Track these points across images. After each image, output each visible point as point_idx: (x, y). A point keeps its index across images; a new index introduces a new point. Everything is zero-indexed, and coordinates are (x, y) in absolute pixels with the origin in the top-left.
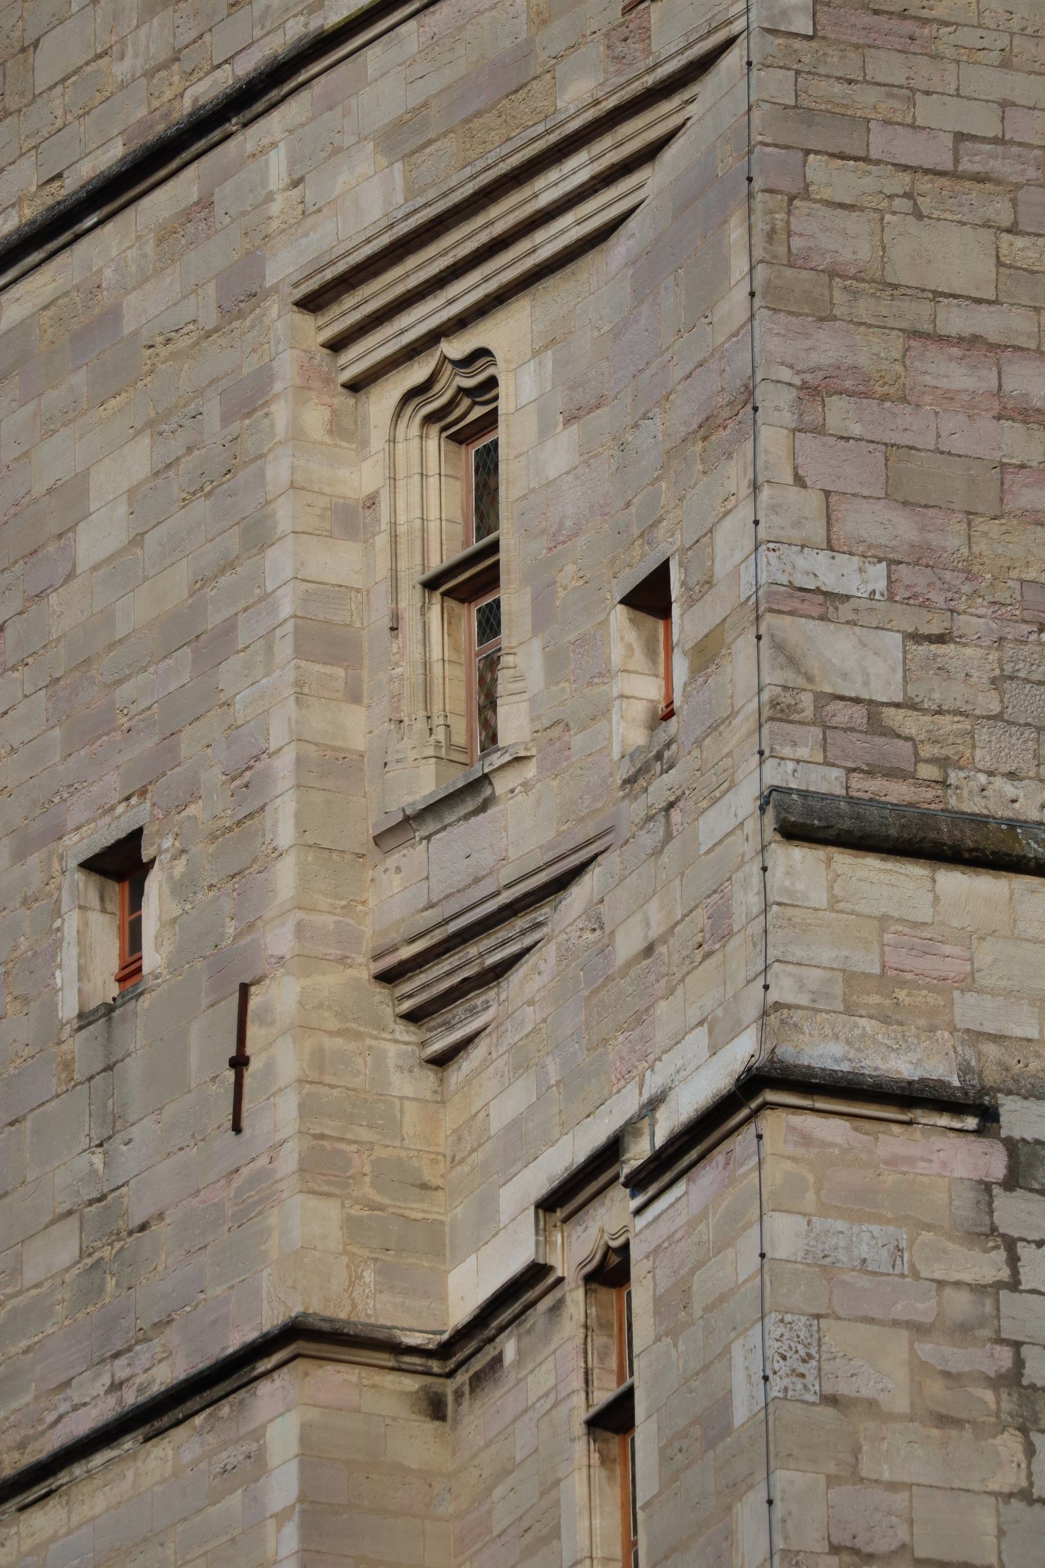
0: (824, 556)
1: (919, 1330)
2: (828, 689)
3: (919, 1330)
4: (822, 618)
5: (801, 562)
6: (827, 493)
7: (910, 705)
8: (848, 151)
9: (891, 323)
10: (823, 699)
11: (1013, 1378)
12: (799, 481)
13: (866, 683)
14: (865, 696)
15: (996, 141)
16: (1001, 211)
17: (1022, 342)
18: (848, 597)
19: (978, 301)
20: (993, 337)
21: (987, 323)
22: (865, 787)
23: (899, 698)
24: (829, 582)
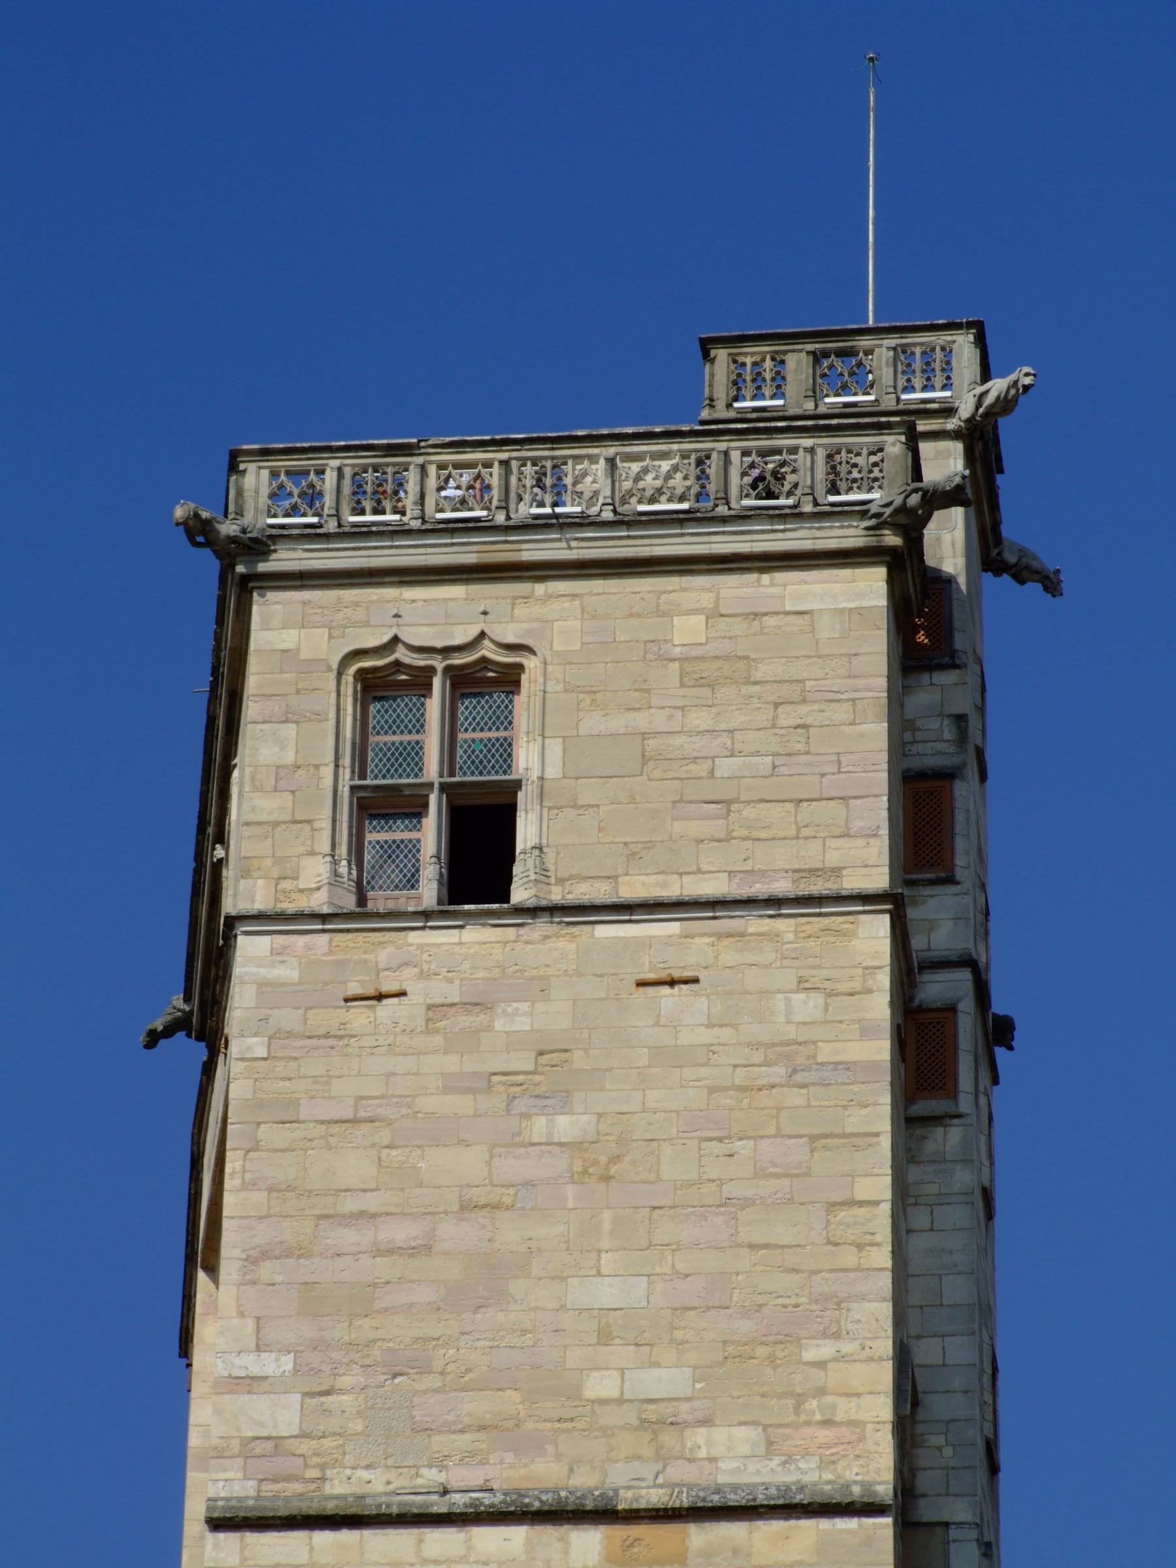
0: (252, 1356)
2: (250, 1434)
4: (249, 1393)
5: (237, 1362)
6: (258, 1319)
7: (304, 1435)
8: (286, 1119)
9: (307, 1212)
10: (247, 1442)
12: (242, 1314)
13: (275, 1427)
14: (275, 1434)
15: (382, 1097)
16: (384, 1136)
17: (392, 1209)
18: (267, 1377)
19: (364, 1191)
20: (373, 1209)
21: (371, 1203)
22: (270, 1489)
23: (296, 1432)
24: (255, 1371)
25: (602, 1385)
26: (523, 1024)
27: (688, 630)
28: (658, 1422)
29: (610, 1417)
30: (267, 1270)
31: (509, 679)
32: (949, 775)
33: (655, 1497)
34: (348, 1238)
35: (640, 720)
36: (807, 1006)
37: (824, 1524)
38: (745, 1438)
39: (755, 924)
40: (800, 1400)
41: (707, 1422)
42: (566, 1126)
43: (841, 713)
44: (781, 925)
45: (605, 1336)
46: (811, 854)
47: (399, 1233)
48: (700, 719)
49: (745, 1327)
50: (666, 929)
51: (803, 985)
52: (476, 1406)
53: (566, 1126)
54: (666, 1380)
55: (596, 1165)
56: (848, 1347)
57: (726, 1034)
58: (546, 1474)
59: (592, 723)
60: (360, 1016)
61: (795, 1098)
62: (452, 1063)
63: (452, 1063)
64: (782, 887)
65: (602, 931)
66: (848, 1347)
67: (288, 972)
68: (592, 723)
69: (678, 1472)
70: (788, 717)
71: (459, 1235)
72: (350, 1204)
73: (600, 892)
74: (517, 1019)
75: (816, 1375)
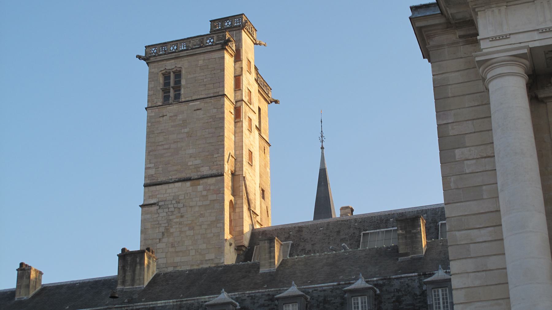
1: (151, 222)
3: (151, 222)
11: (158, 224)
21: (163, 143)
25: (190, 163)
26: (181, 117)
27: (201, 62)
28: (197, 168)
29: (191, 167)
30: (151, 153)
31: (180, 71)
32: (240, 76)
33: (196, 177)
34: (160, 148)
35: (195, 75)
36: (215, 111)
37: (216, 178)
38: (207, 168)
39: (208, 100)
40: (213, 162)
41: (203, 167)
42: (186, 130)
43: (219, 71)
44: (212, 100)
45: (191, 157)
46: (215, 90)
47: (166, 147)
48: (202, 74)
49: (207, 154)
50: (197, 103)
51: (214, 108)
52: (175, 168)
53: (186, 130)
54: (198, 162)
55: (189, 135)
56: (219, 155)
57: (205, 116)
58: (183, 175)
59: (189, 76)
60: (161, 119)
61: (213, 123)
62: (172, 124)
63: (172, 124)
64: (212, 95)
65: (190, 104)
66: (219, 155)
67: (153, 114)
68: (189, 76)
69: (199, 173)
70: (213, 72)
71: (173, 146)
72: (160, 144)
73: (190, 99)
74: (180, 117)
75: (215, 159)
